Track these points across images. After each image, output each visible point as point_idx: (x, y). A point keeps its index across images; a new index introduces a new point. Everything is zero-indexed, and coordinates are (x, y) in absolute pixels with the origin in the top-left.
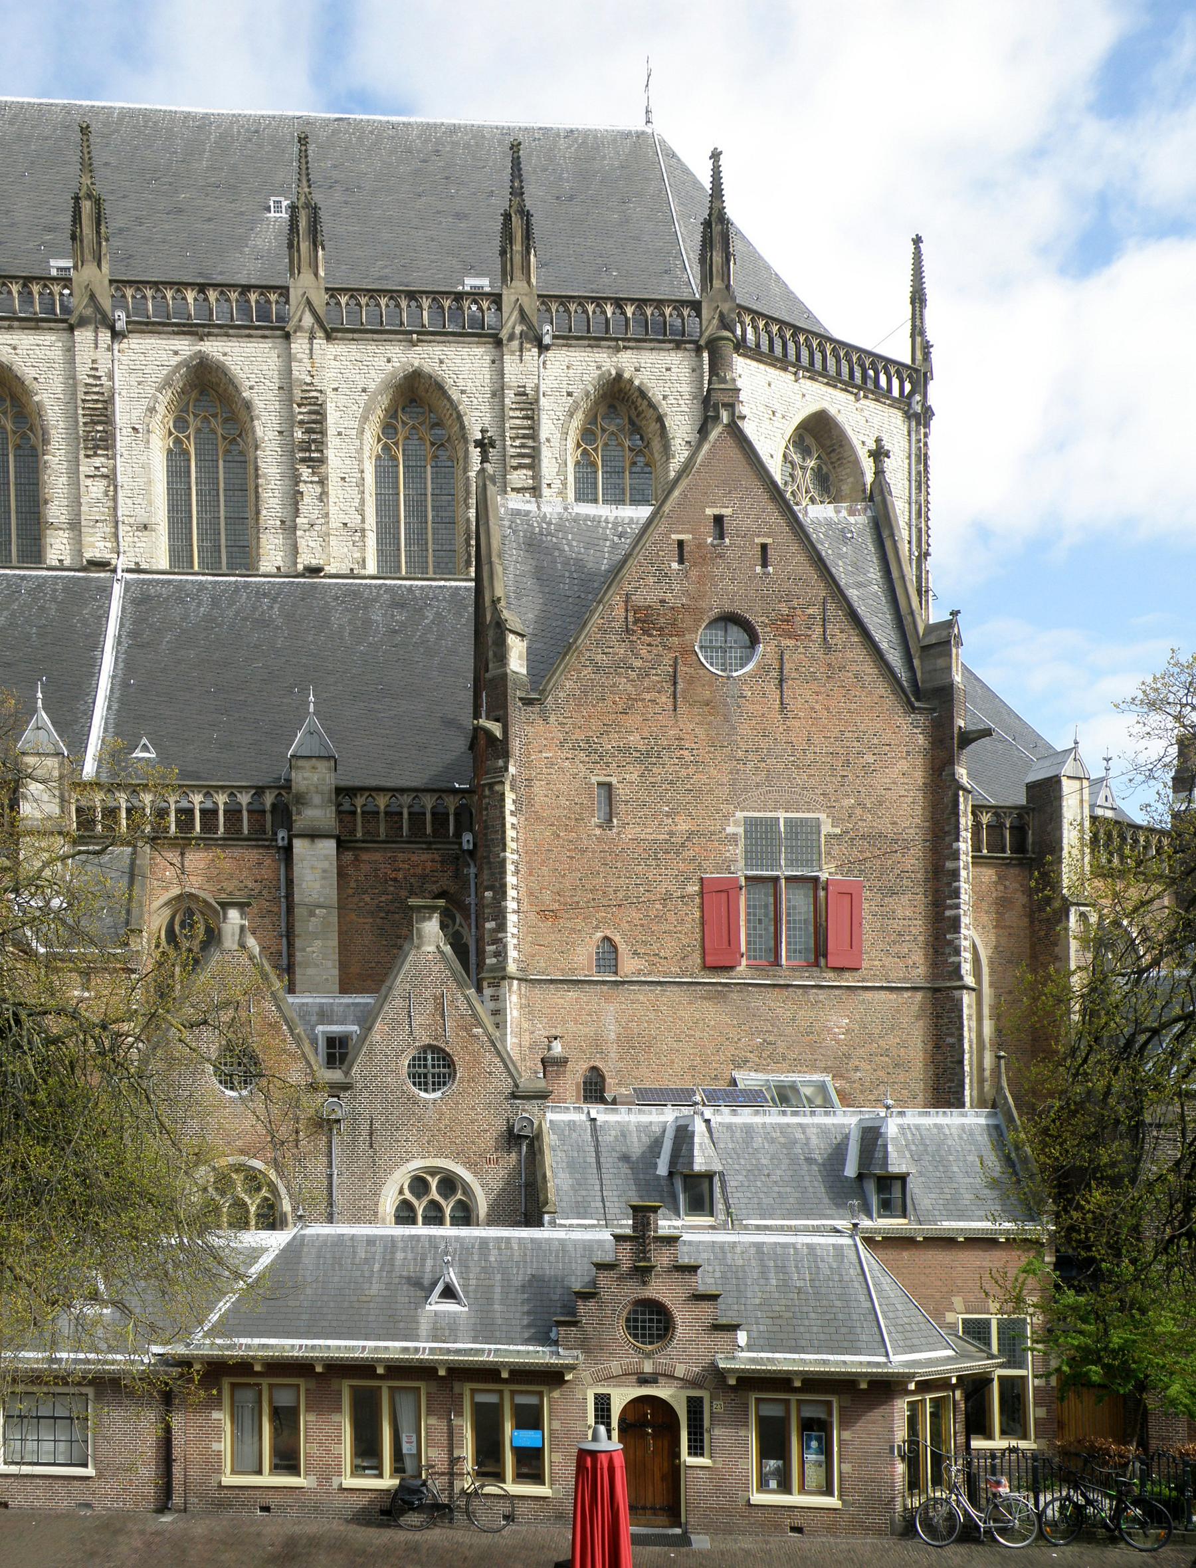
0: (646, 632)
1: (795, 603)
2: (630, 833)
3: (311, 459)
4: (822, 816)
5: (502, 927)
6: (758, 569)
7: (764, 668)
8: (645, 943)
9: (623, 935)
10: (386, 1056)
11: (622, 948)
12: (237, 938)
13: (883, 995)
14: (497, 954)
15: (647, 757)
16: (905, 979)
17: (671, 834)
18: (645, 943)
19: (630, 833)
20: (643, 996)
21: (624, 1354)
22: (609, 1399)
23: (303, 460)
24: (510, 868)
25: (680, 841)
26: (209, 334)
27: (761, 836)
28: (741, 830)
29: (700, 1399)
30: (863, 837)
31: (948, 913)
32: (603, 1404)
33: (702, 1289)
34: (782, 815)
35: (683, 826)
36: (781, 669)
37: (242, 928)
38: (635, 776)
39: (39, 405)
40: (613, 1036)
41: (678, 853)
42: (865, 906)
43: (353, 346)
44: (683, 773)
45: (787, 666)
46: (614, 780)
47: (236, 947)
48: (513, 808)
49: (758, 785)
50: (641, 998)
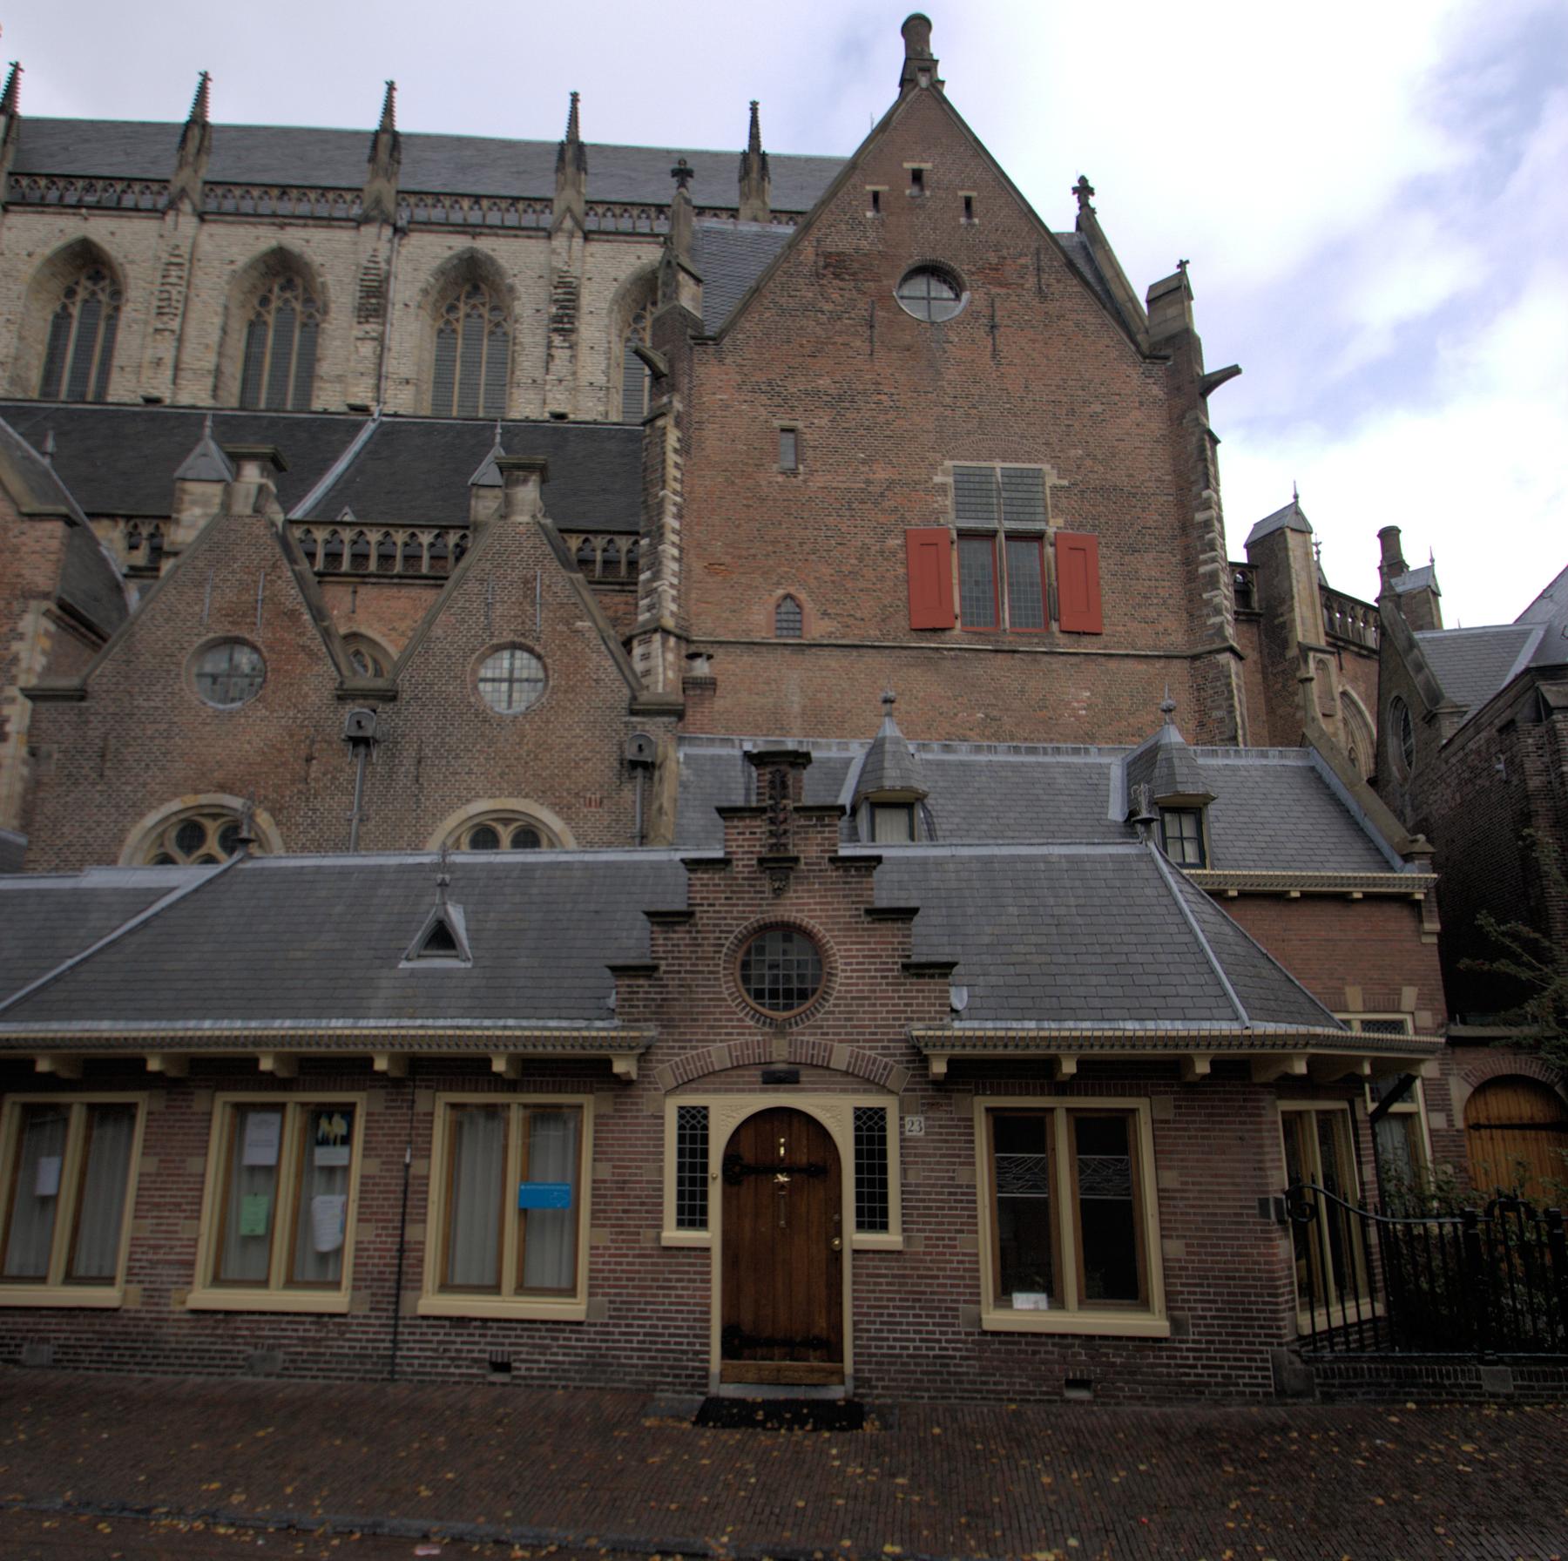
0: (837, 276)
1: (1005, 252)
2: (818, 481)
3: (563, 329)
4: (1046, 467)
5: (657, 576)
6: (963, 220)
7: (972, 314)
8: (837, 601)
9: (811, 593)
10: (449, 657)
11: (809, 606)
12: (252, 500)
13: (1130, 665)
14: (650, 608)
15: (840, 401)
16: (1155, 648)
17: (868, 482)
18: (837, 601)
19: (818, 481)
20: (833, 660)
21: (735, 1031)
22: (706, 1117)
23: (556, 330)
24: (671, 509)
25: (878, 490)
26: (481, 234)
27: (971, 487)
28: (950, 480)
29: (879, 1114)
30: (1095, 490)
31: (1203, 569)
32: (694, 1125)
33: (883, 900)
34: (999, 465)
35: (882, 474)
36: (992, 317)
37: (261, 489)
38: (824, 422)
39: (324, 284)
40: (796, 708)
41: (876, 503)
42: (1103, 564)
43: (607, 246)
44: (881, 419)
45: (998, 313)
46: (800, 425)
47: (248, 511)
48: (677, 446)
49: (969, 433)
50: (833, 664)
